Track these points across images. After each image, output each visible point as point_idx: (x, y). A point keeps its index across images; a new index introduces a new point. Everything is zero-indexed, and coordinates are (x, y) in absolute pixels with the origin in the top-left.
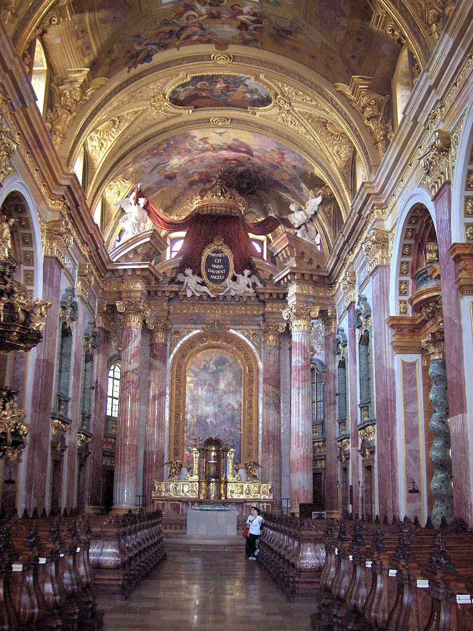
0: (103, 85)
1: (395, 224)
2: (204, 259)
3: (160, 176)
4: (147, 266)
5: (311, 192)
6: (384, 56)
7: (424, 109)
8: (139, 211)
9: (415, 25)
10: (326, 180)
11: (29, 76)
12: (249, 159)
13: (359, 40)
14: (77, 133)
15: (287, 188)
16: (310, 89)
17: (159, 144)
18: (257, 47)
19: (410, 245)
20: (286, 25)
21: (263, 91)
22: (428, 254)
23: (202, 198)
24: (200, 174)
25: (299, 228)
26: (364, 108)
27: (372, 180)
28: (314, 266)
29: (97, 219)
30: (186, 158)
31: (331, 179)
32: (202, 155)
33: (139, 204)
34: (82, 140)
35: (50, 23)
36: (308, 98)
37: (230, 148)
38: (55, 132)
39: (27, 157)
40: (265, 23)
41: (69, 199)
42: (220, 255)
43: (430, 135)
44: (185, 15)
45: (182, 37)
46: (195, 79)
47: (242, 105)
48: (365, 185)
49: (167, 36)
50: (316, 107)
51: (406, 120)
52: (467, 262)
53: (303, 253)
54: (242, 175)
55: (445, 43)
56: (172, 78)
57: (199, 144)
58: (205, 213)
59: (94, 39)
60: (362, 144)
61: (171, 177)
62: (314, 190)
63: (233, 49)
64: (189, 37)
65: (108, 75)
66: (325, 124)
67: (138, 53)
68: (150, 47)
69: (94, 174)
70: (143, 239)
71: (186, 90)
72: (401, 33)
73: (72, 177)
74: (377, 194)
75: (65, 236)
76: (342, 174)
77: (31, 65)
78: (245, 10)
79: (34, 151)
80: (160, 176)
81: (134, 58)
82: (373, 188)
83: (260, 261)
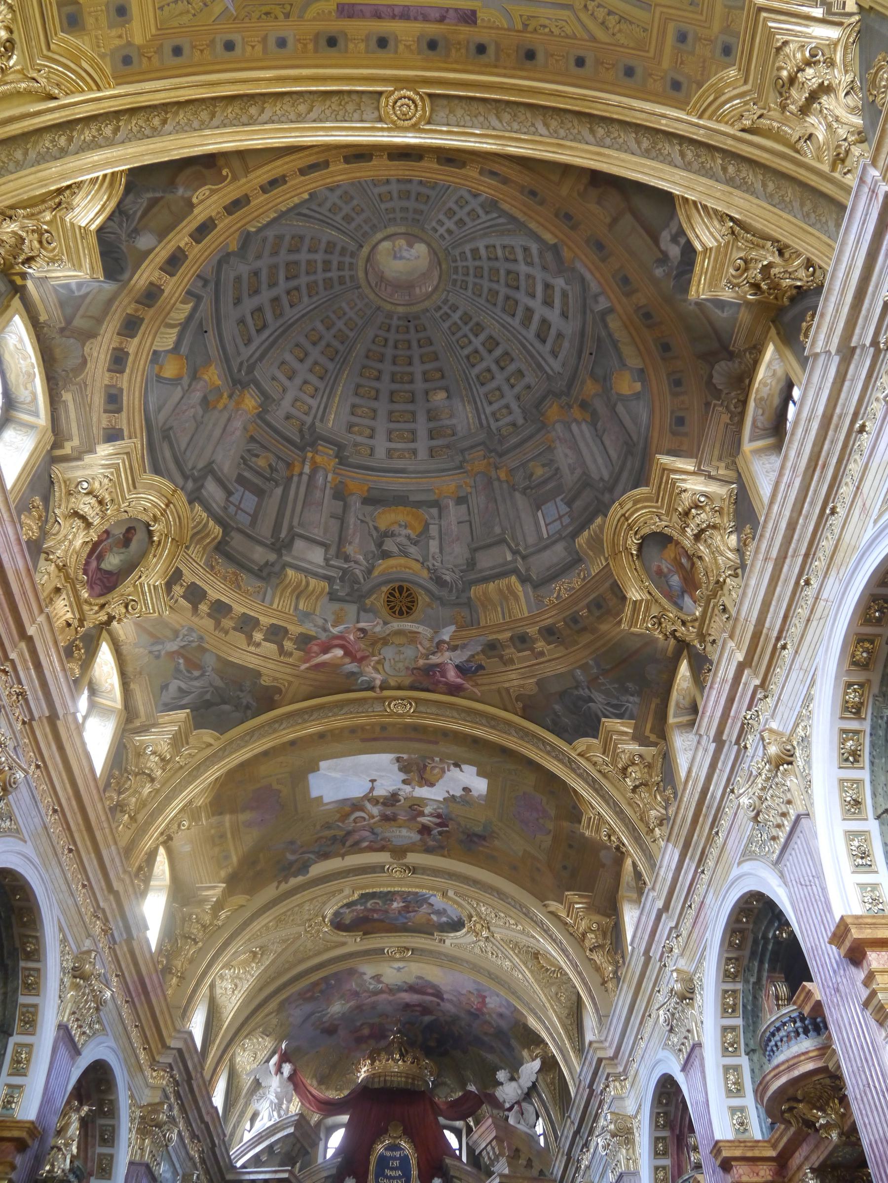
0: (243, 906)
1: (640, 1105)
2: (373, 1159)
4: (286, 1175)
5: (525, 1053)
6: (603, 866)
7: (656, 939)
8: (281, 1083)
9: (634, 829)
10: (544, 1035)
11: (142, 894)
12: (438, 1004)
13: (571, 846)
14: (200, 971)
17: (315, 984)
19: (664, 1138)
20: (478, 829)
21: (454, 912)
22: (692, 1154)
23: (372, 1064)
25: (510, 1109)
26: (584, 935)
27: (603, 1038)
28: (535, 1172)
29: (218, 1100)
30: (352, 1003)
31: (551, 1034)
32: (374, 999)
34: (208, 981)
35: (179, 826)
36: (512, 922)
37: (411, 989)
38: (171, 969)
39: (125, 1011)
40: (452, 826)
41: (179, 1070)
42: (397, 1154)
43: (669, 974)
45: (348, 844)
46: (365, 897)
47: (426, 929)
48: (595, 1045)
50: (523, 932)
51: (636, 953)
52: (741, 1171)
53: (517, 1150)
54: (430, 1028)
55: (670, 856)
56: (334, 896)
58: (376, 1086)
59: (236, 848)
60: (585, 984)
61: (330, 1031)
62: (529, 1049)
63: (413, 858)
65: (251, 891)
66: (536, 955)
67: (291, 864)
70: (284, 1129)
71: (353, 911)
72: (619, 838)
73: (186, 1036)
74: (611, 1059)
75: (166, 1127)
76: (564, 1026)
77: (147, 880)
78: (427, 810)
79: (136, 1000)
81: (287, 870)
82: (604, 1049)
83: (456, 1163)
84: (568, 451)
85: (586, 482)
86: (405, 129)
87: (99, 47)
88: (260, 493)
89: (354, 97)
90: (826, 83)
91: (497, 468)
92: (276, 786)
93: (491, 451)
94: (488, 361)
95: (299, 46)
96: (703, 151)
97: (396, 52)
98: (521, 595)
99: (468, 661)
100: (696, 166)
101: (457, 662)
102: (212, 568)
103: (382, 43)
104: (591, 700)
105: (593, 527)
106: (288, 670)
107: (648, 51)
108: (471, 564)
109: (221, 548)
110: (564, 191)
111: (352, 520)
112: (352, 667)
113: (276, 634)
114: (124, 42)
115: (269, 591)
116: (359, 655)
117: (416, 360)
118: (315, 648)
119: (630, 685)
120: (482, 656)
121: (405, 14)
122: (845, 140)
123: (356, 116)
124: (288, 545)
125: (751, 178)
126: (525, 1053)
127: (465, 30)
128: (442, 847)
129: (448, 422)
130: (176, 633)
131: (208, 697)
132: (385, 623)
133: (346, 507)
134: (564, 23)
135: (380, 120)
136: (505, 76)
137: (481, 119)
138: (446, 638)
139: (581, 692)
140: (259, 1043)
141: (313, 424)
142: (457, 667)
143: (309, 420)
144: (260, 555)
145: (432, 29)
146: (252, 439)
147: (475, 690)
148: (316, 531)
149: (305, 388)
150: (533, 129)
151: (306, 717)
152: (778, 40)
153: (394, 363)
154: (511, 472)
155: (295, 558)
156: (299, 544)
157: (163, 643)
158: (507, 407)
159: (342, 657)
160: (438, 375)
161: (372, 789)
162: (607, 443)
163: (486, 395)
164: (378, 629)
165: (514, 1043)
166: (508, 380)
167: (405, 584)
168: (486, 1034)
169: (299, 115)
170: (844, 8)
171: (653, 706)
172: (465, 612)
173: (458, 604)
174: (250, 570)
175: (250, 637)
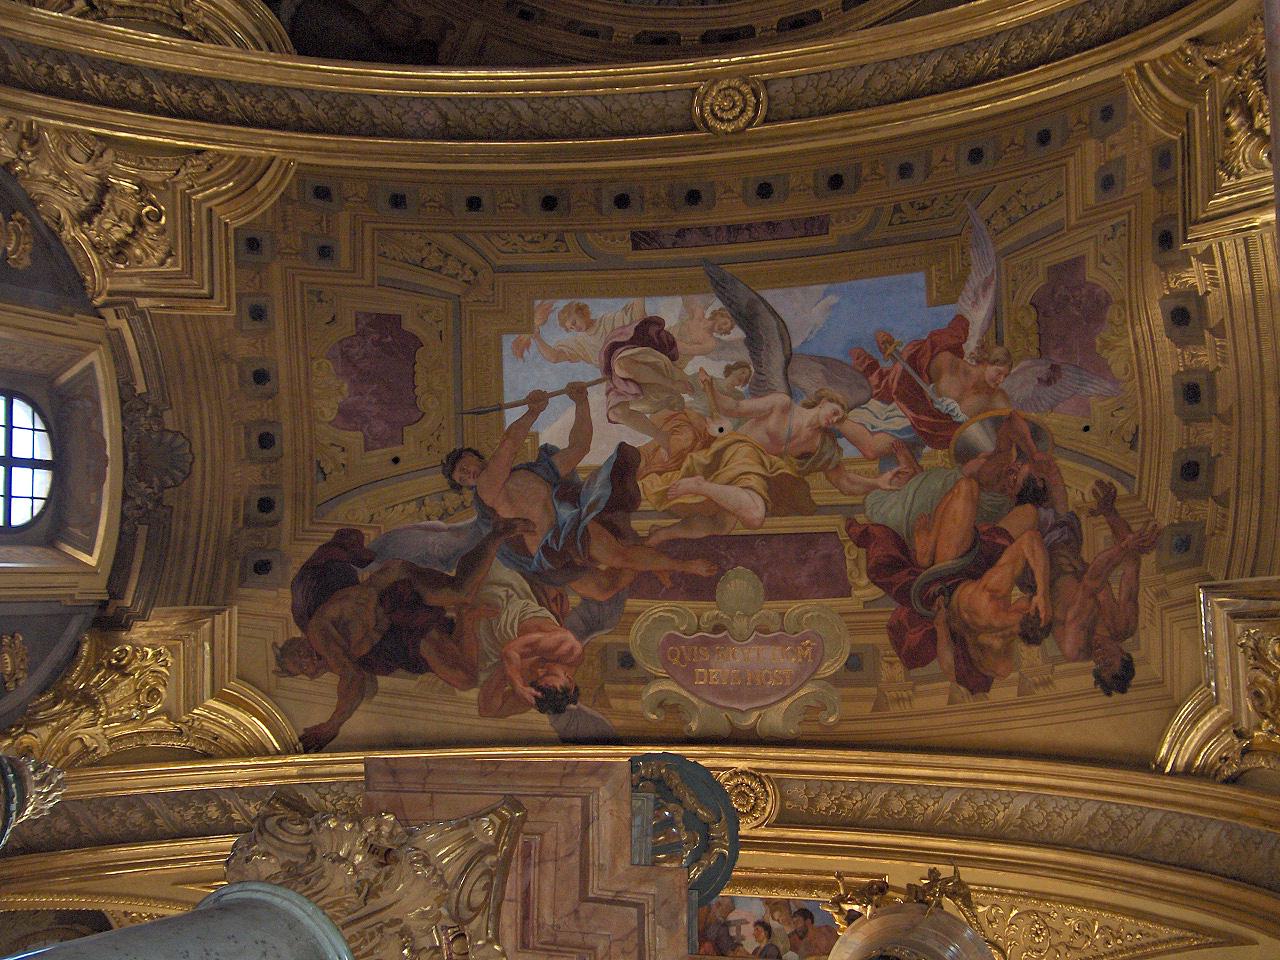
86: (727, 75)
87: (1140, 128)
89: (804, 110)
90: (86, 225)
95: (881, 170)
96: (263, 117)
97: (746, 180)
100: (270, 96)
103: (765, 191)
107: (374, 229)
110: (476, 28)
114: (1110, 140)
121: (734, 232)
122: (28, 163)
123: (802, 84)
125: (174, 93)
127: (647, 221)
134: (504, 249)
135: (766, 82)
136: (584, 171)
137: (616, 108)
145: (695, 217)
150: (535, 106)
152: (174, 264)
169: (883, 72)
170: (116, 311)
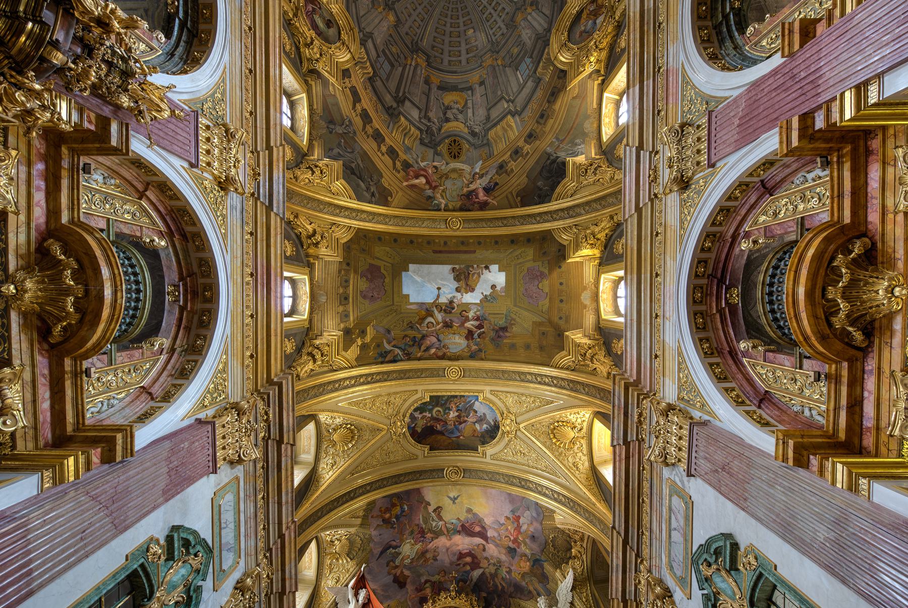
3: (389, 574)
5: (558, 574)
12: (484, 550)
13: (561, 301)
15: (530, 592)
16: (532, 385)
18: (482, 359)
20: (502, 323)
24: (433, 584)
33: (358, 601)
44: (426, 322)
45: (423, 348)
49: (411, 343)
57: (433, 520)
62: (561, 569)
64: (428, 349)
67: (387, 353)
68: (397, 351)
69: (317, 490)
78: (471, 314)
80: (389, 574)
84: (528, 31)
85: (538, 37)
88: (392, 66)
91: (497, 60)
92: (382, 270)
93: (493, 52)
94: (490, 10)
98: (513, 124)
99: (490, 182)
101: (484, 185)
102: (366, 89)
104: (558, 157)
105: (545, 56)
106: (397, 182)
108: (488, 118)
109: (371, 80)
111: (432, 98)
112: (429, 192)
113: (392, 153)
115: (391, 124)
116: (434, 184)
117: (461, 17)
118: (411, 173)
119: (578, 141)
120: (496, 176)
124: (403, 102)
126: (558, 574)
128: (480, 350)
129: (474, 44)
130: (343, 120)
131: (353, 165)
132: (447, 164)
133: (430, 89)
138: (477, 170)
139: (552, 158)
140: (343, 564)
141: (417, 41)
142: (484, 189)
143: (416, 39)
144: (388, 99)
146: (391, 35)
147: (495, 202)
148: (415, 99)
149: (415, 22)
151: (404, 222)
153: (452, 19)
154: (503, 59)
155: (405, 111)
156: (407, 103)
157: (335, 124)
158: (499, 27)
159: (425, 185)
160: (470, 22)
161: (438, 296)
162: (544, 10)
163: (490, 26)
164: (443, 167)
165: (548, 567)
166: (498, 15)
167: (457, 139)
168: (523, 575)
171: (593, 145)
172: (486, 150)
173: (483, 145)
174: (383, 105)
175: (379, 147)
